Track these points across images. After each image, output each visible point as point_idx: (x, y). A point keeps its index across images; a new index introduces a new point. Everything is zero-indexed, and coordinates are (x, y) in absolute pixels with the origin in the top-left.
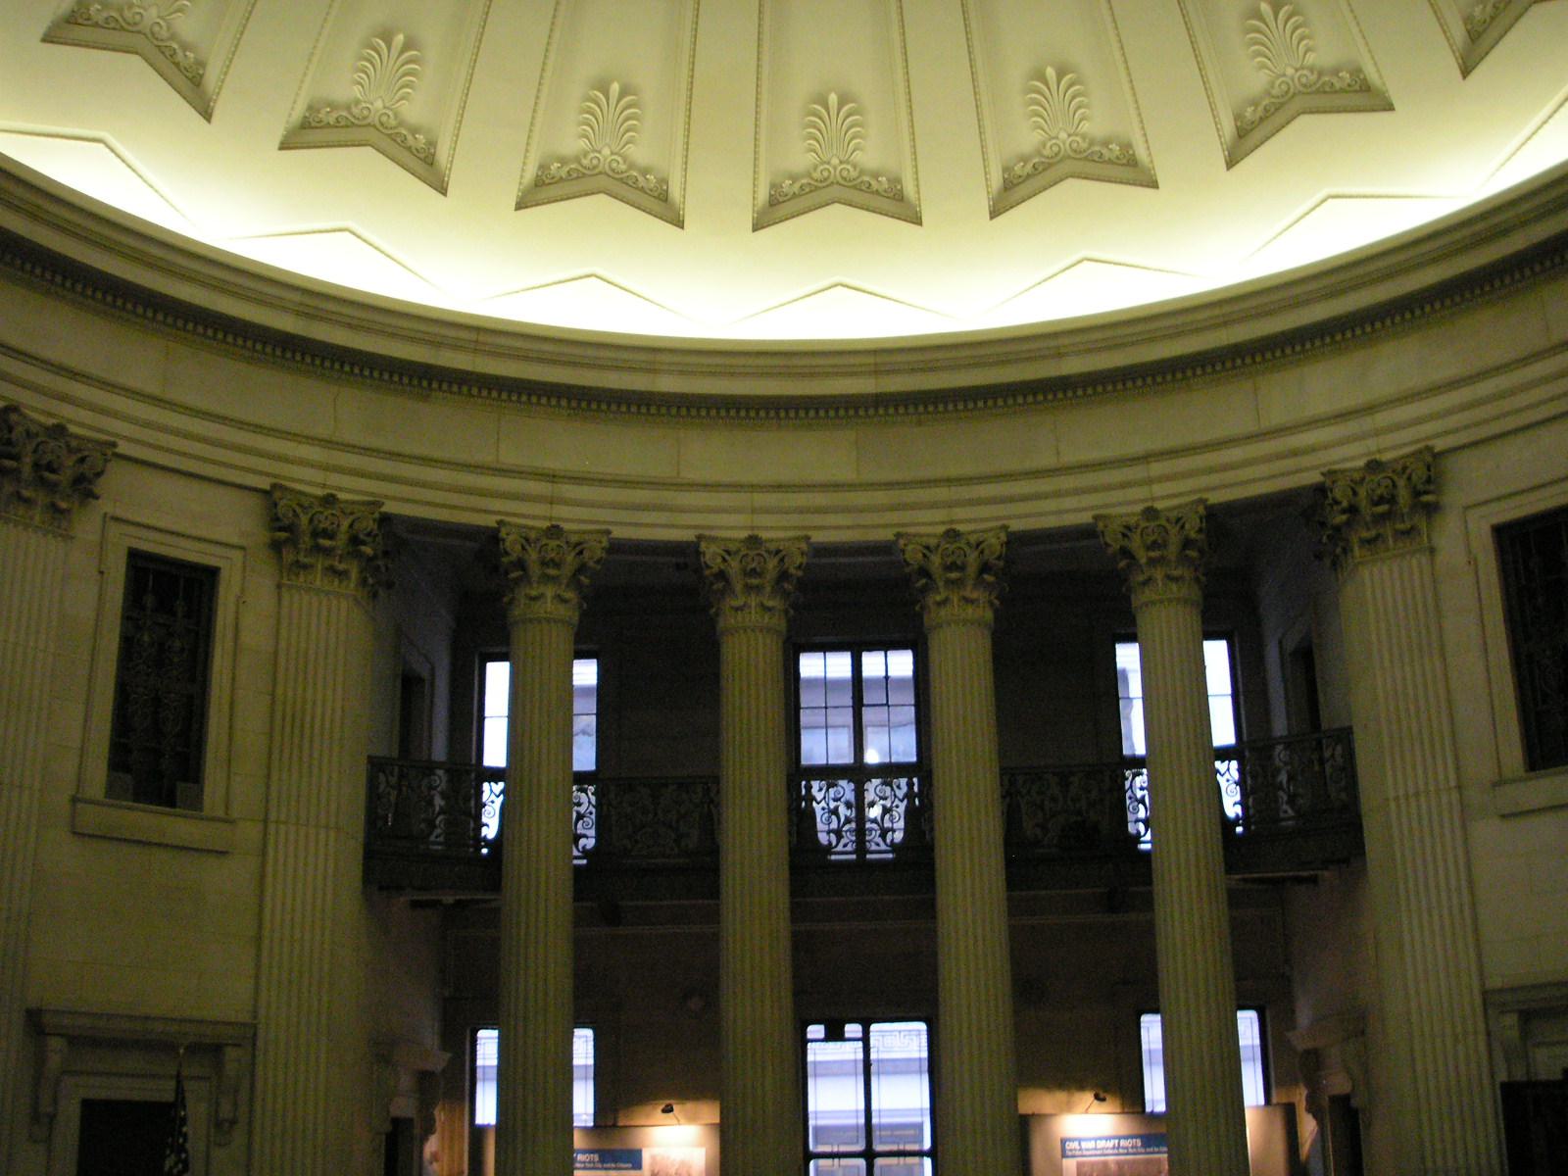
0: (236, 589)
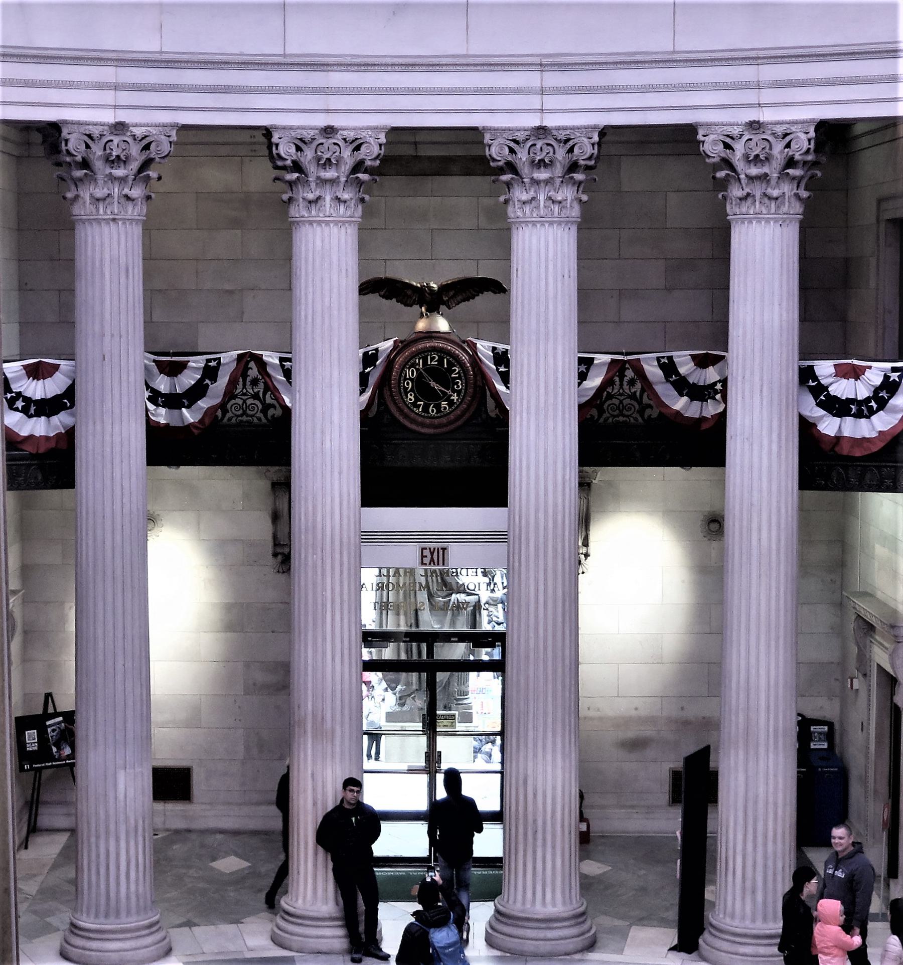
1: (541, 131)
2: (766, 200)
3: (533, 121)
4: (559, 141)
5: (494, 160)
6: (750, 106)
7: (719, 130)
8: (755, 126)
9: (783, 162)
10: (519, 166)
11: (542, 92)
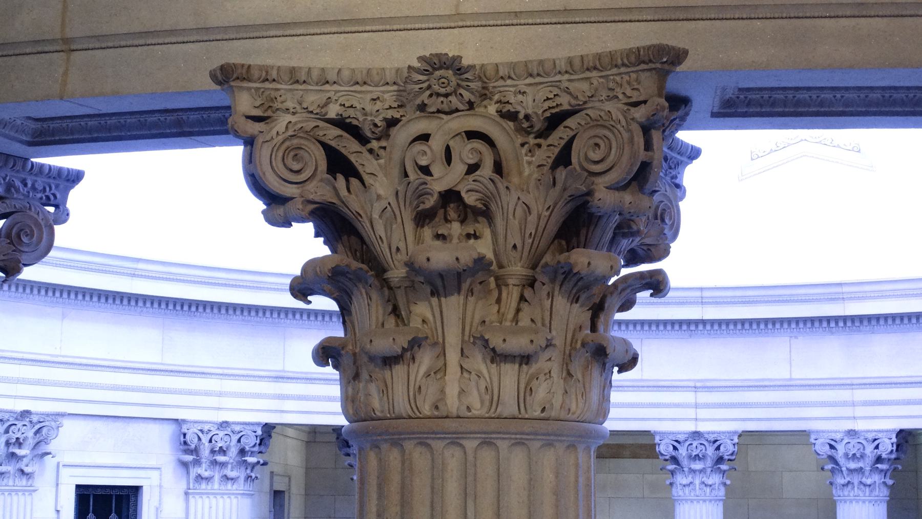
0: (154, 502)
1: (696, 435)
2: (862, 487)
3: (690, 427)
4: (710, 442)
5: (662, 455)
6: (848, 418)
7: (826, 435)
8: (852, 433)
9: (874, 459)
10: (680, 459)
11: (696, 406)
